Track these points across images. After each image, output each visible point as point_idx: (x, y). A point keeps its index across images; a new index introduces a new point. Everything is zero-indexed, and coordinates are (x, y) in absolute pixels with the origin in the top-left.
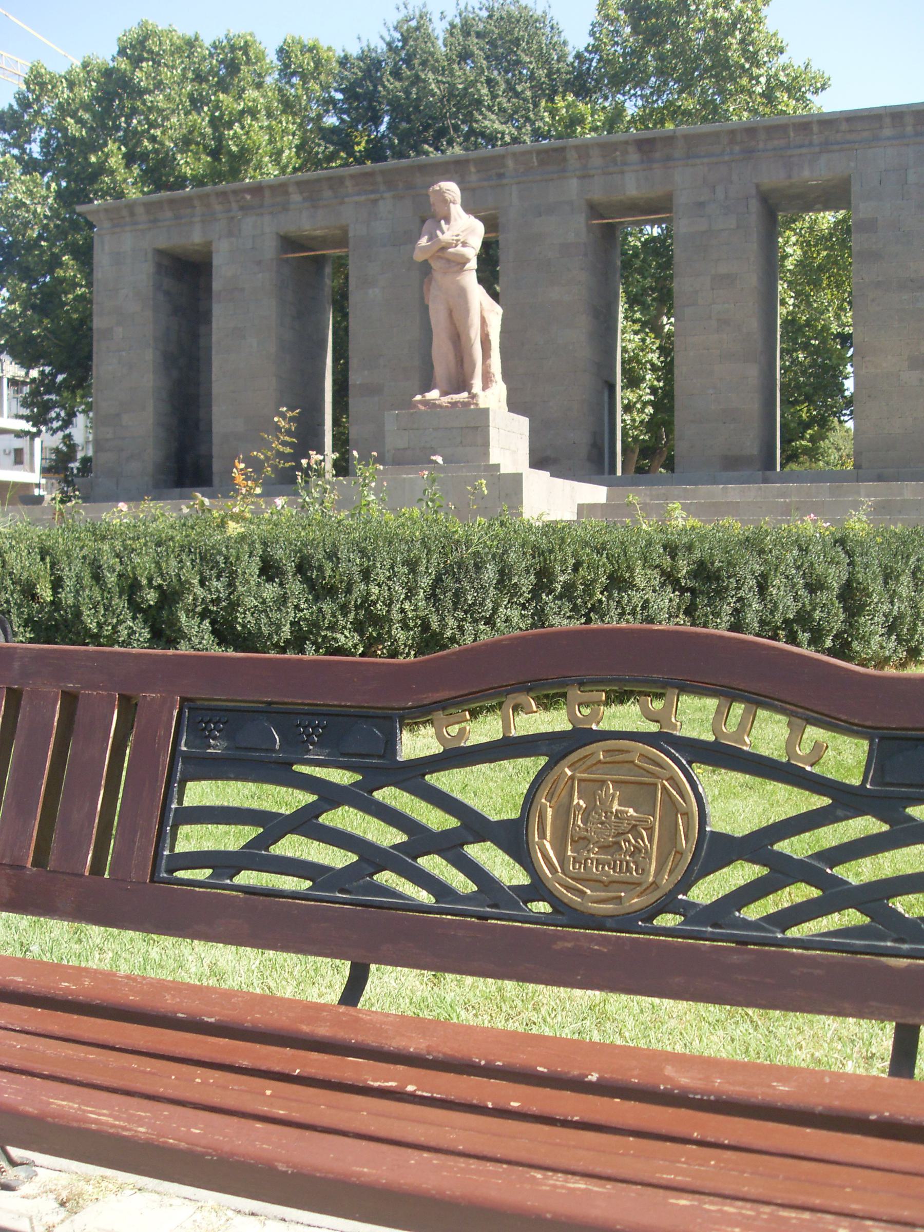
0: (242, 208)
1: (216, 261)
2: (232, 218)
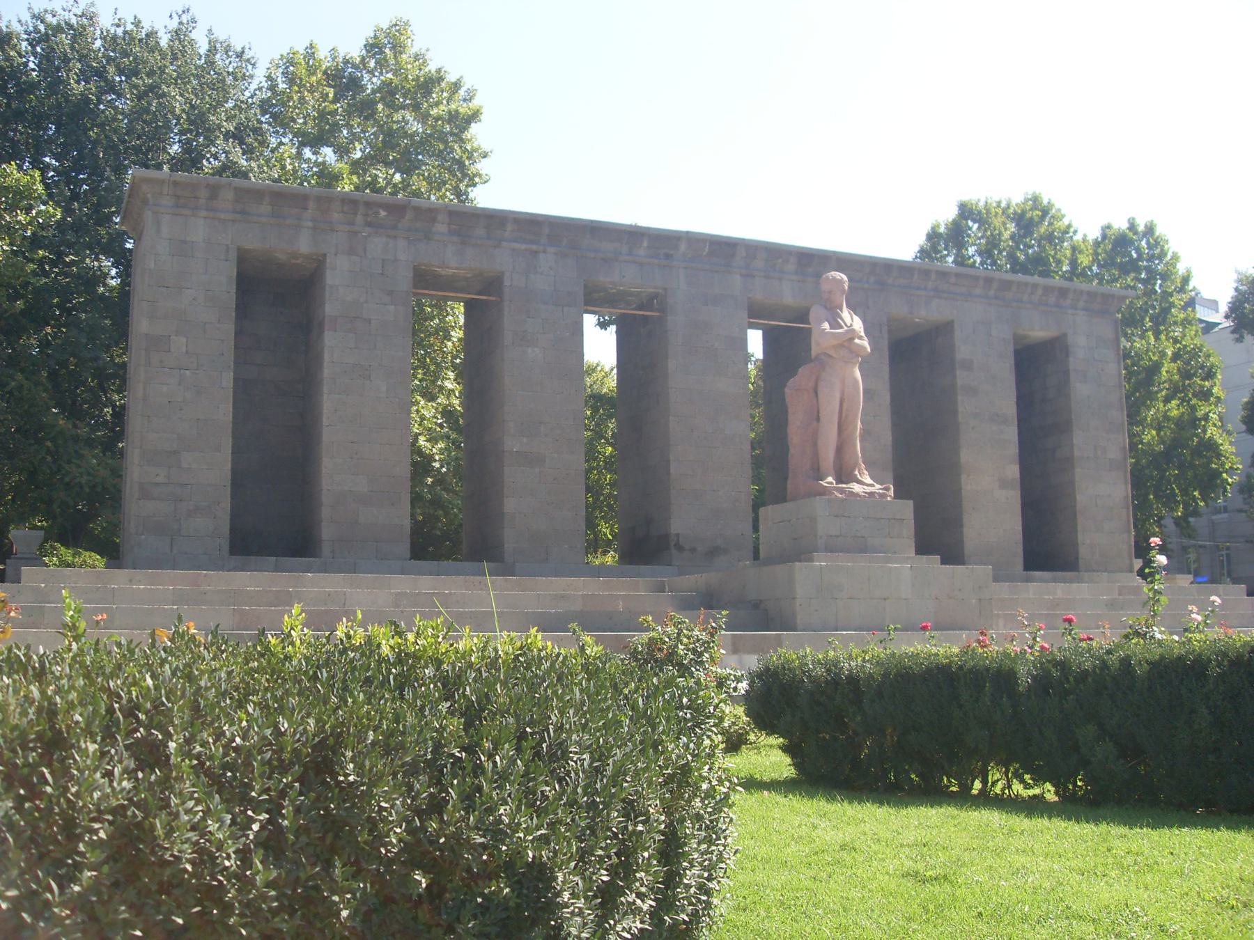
0: (369, 224)
2: (356, 233)
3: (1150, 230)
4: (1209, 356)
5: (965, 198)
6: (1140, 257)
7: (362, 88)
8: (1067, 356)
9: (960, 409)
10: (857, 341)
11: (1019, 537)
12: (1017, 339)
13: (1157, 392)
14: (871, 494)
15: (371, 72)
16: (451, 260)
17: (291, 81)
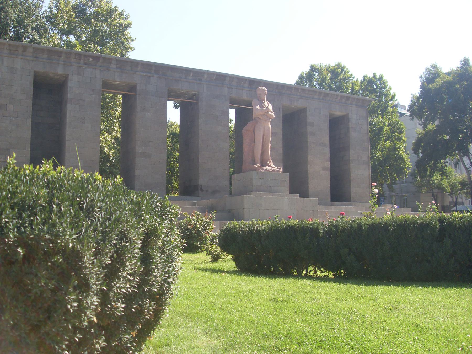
0: (85, 64)
1: (71, 84)
2: (80, 67)
3: (381, 78)
4: (401, 125)
5: (313, 64)
6: (377, 88)
7: (86, 13)
8: (349, 122)
9: (308, 140)
10: (270, 113)
11: (329, 189)
12: (330, 115)
13: (382, 138)
14: (274, 170)
15: (90, 7)
16: (117, 78)
17: (58, 9)
